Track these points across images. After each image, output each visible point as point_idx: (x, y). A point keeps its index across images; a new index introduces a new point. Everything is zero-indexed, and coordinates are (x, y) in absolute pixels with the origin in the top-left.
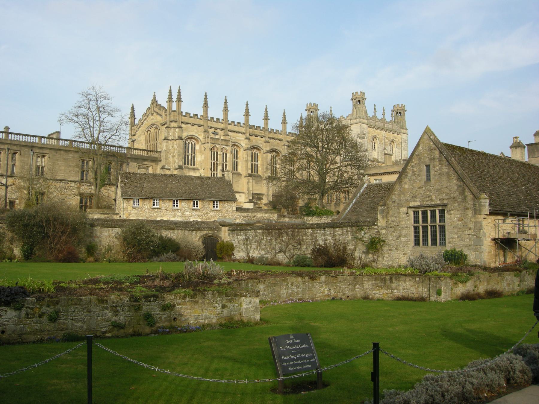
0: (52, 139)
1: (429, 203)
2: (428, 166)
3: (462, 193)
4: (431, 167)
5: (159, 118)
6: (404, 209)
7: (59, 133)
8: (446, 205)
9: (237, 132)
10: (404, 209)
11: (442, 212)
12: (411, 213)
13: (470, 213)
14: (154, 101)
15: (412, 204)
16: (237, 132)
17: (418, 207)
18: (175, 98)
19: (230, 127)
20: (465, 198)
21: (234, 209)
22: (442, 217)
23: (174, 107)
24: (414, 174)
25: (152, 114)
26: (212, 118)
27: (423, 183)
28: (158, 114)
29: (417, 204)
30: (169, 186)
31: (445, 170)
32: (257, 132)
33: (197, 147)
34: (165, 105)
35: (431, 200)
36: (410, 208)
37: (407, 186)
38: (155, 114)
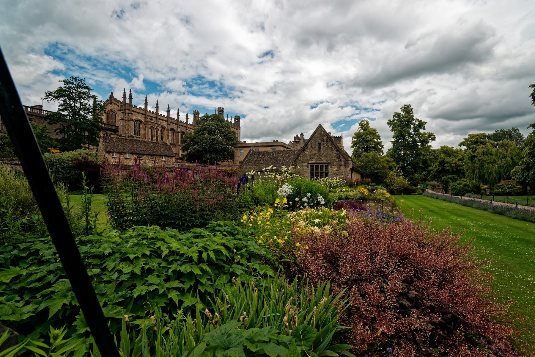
0: (35, 109)
1: (320, 162)
2: (319, 144)
3: (339, 157)
4: (322, 144)
5: (116, 107)
6: (306, 164)
7: (42, 106)
8: (330, 163)
9: (163, 120)
10: (306, 164)
11: (327, 167)
12: (310, 166)
13: (342, 168)
14: (112, 96)
15: (310, 162)
16: (163, 120)
17: (314, 163)
18: (128, 96)
19: (159, 117)
20: (340, 161)
21: (174, 160)
22: (327, 168)
23: (127, 101)
24: (312, 147)
25: (111, 104)
26: (150, 111)
27: (317, 152)
28: (115, 104)
29: (313, 162)
30: (135, 146)
31: (330, 146)
32: (173, 121)
33: (141, 126)
34: (121, 100)
35: (322, 160)
36: (309, 164)
37: (307, 153)
38: (113, 104)
